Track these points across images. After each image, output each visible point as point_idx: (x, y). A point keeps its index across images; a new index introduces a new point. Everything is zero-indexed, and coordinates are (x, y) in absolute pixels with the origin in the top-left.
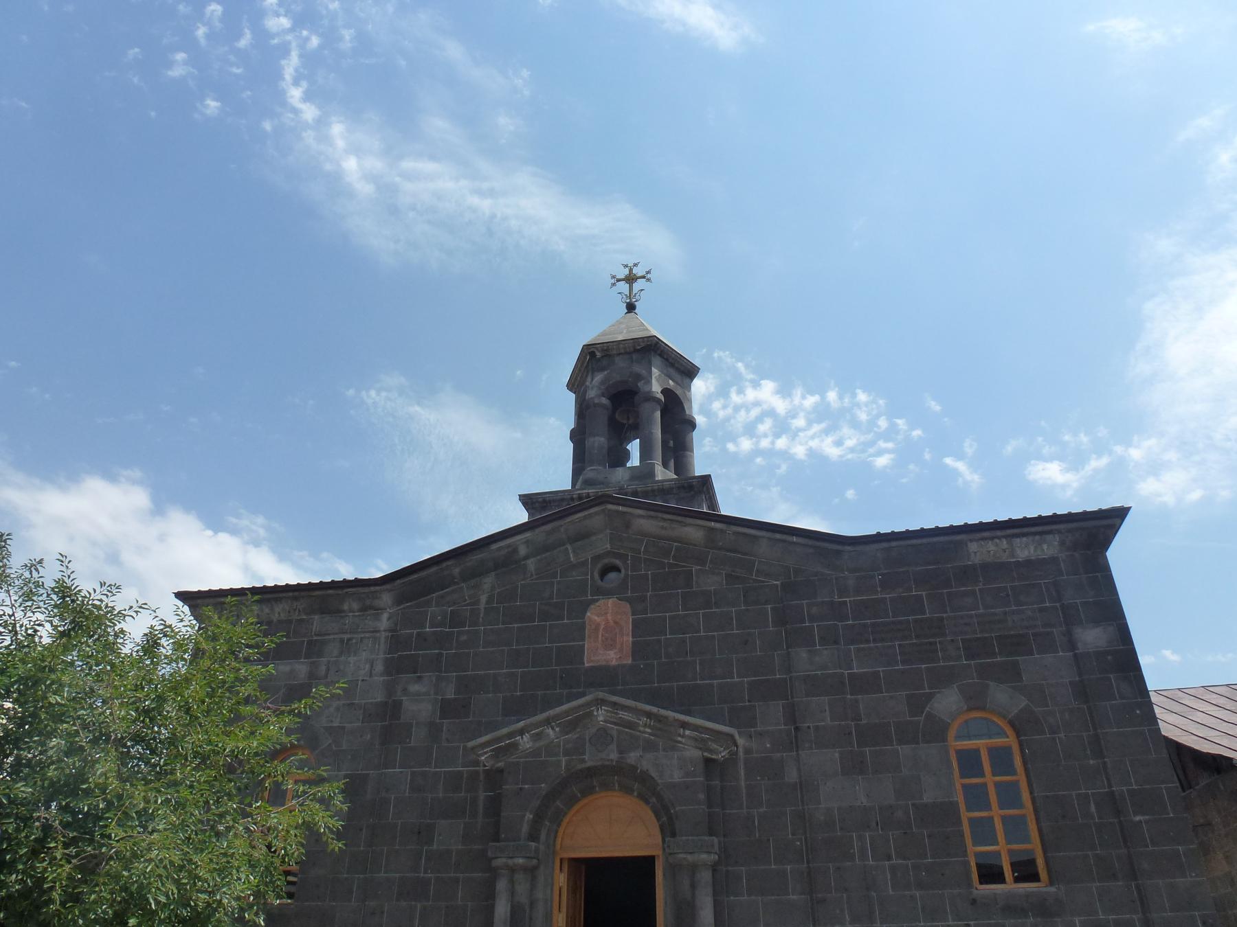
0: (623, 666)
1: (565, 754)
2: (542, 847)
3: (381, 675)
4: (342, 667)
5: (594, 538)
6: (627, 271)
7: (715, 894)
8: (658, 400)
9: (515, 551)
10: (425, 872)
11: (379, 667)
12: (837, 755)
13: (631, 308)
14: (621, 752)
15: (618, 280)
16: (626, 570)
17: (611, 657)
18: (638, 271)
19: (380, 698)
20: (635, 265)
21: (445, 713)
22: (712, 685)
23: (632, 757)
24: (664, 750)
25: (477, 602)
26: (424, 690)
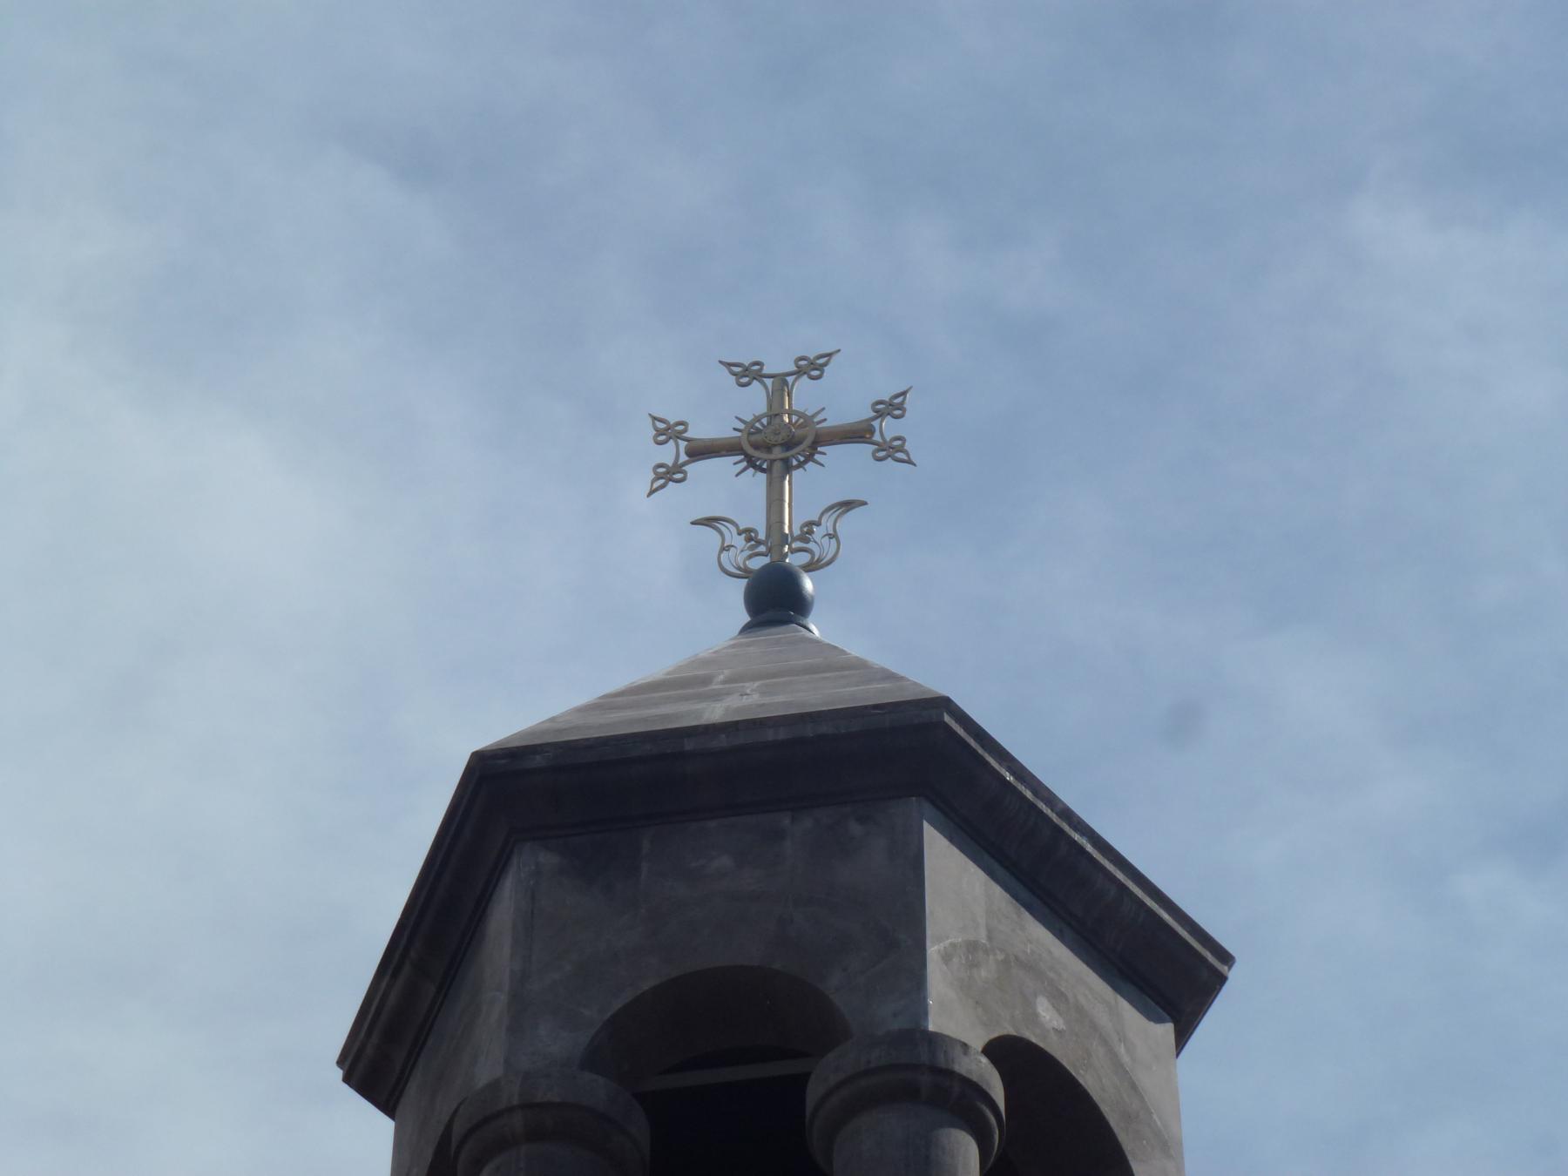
6: (754, 400)
8: (962, 1102)
13: (775, 599)
20: (811, 367)
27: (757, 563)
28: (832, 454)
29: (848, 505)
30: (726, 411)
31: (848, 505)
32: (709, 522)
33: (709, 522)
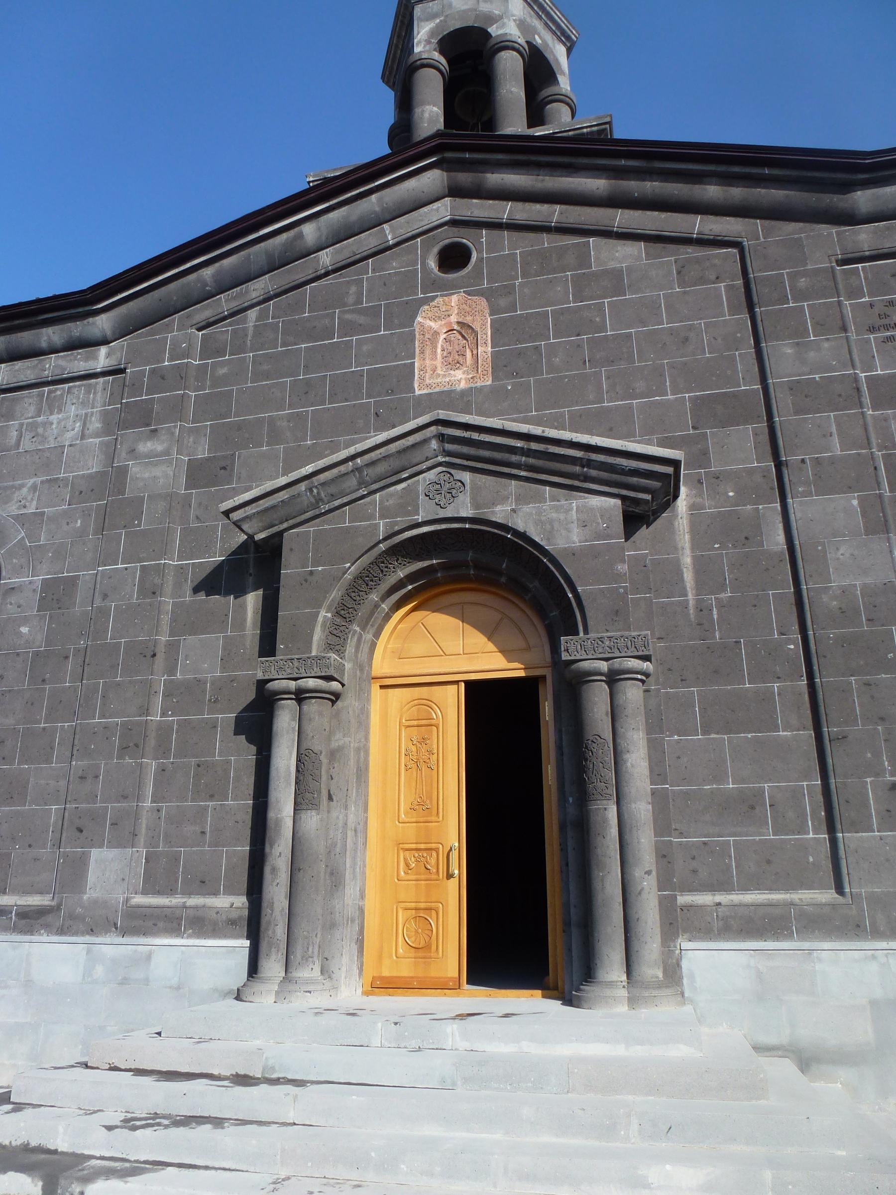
0: (480, 390)
1: (382, 517)
2: (348, 666)
3: (97, 435)
4: (40, 430)
5: (425, 209)
7: (650, 730)
9: (301, 236)
10: (163, 714)
11: (96, 424)
12: (855, 502)
14: (476, 505)
16: (480, 251)
17: (460, 379)
19: (94, 466)
21: (192, 483)
22: (630, 407)
23: (499, 513)
24: (553, 498)
25: (245, 321)
26: (160, 448)
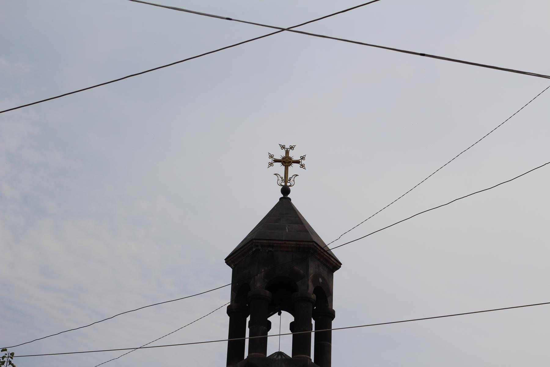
13: (286, 191)
15: (276, 161)
18: (294, 155)
20: (292, 148)
27: (283, 184)
28: (294, 165)
29: (297, 175)
30: (280, 154)
31: (297, 175)
32: (275, 174)
33: (275, 174)
